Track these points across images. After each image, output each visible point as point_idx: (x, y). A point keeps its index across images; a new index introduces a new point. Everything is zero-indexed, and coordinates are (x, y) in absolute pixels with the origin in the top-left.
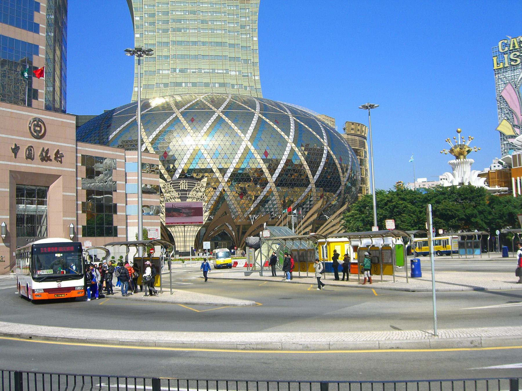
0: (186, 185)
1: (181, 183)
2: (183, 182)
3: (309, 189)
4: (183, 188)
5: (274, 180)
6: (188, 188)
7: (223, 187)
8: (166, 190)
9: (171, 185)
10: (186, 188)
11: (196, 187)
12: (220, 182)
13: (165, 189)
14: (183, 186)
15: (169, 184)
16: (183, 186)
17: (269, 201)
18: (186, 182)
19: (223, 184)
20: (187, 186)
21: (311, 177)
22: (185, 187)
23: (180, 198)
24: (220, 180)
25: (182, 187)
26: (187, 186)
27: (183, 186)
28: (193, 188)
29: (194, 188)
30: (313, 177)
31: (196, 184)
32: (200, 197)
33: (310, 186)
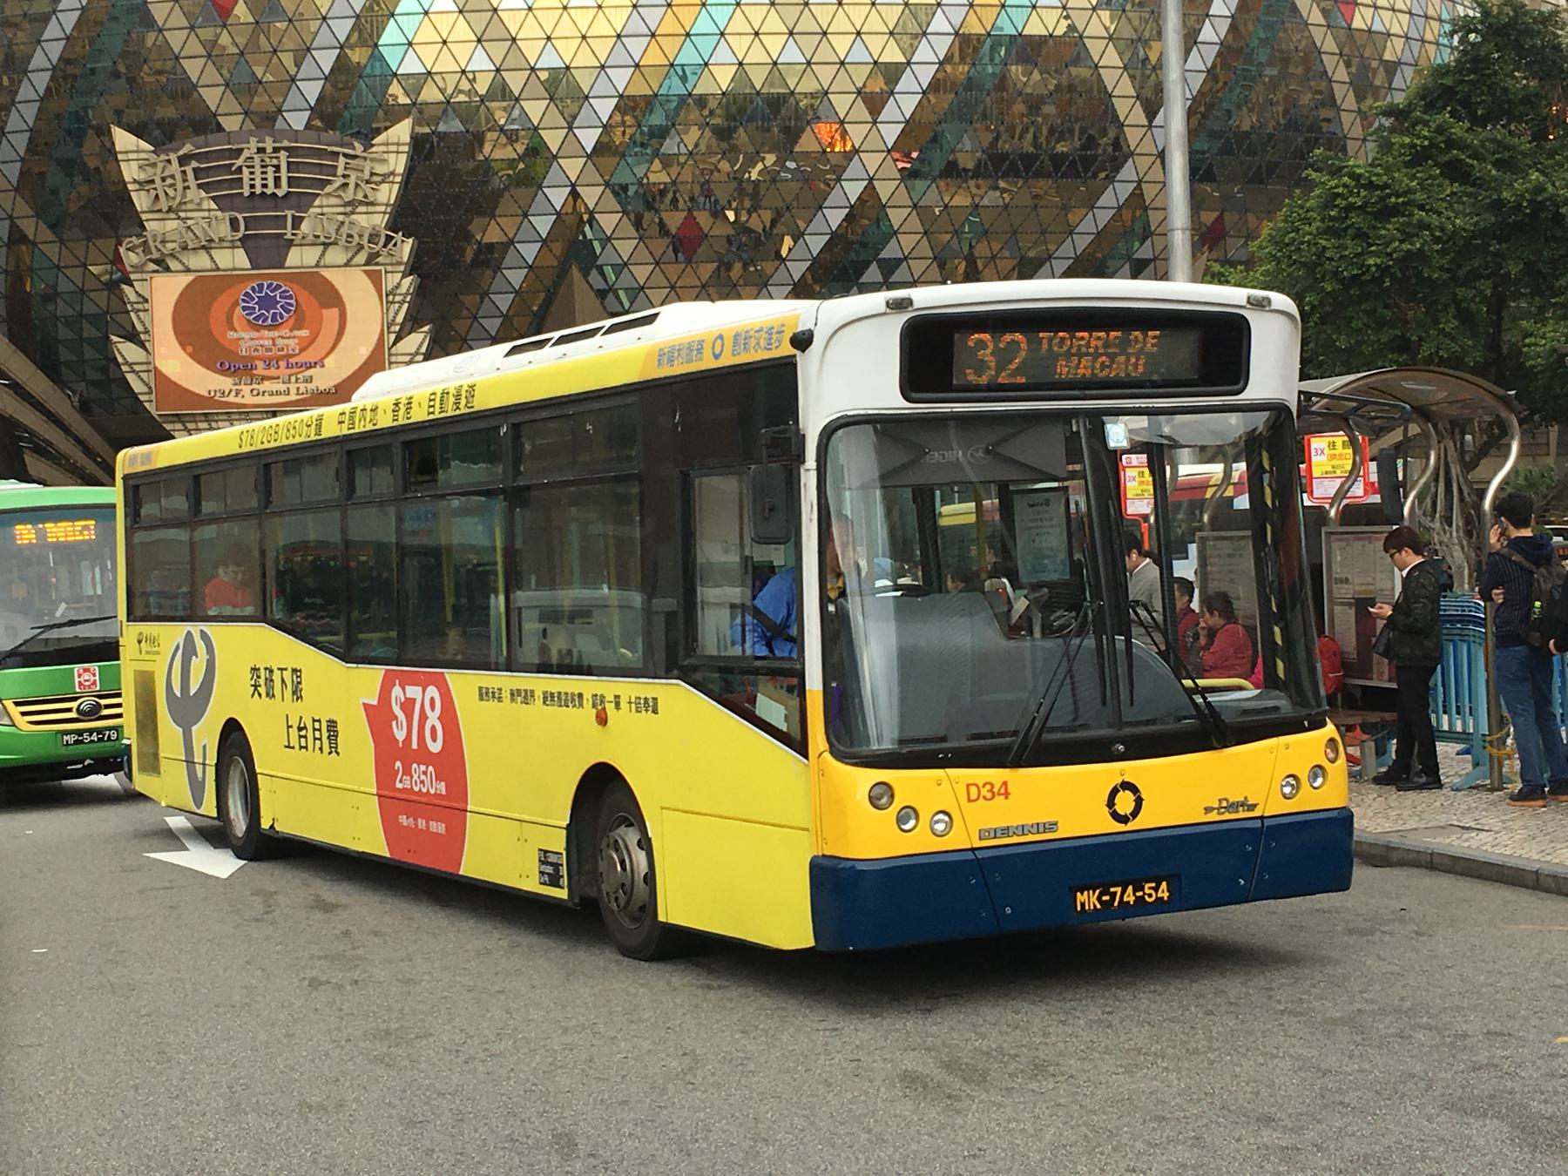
0: (277, 168)
1: (246, 154)
2: (261, 150)
3: (1124, 191)
4: (258, 183)
5: (891, 133)
6: (291, 181)
7: (573, 186)
8: (157, 196)
9: (189, 169)
10: (277, 180)
11: (339, 182)
12: (555, 157)
13: (153, 193)
14: (258, 170)
15: (175, 163)
16: (258, 176)
17: (867, 264)
18: (276, 150)
19: (573, 167)
20: (284, 174)
21: (1139, 116)
22: (271, 182)
23: (244, 241)
24: (553, 139)
25: (254, 179)
26: (284, 174)
27: (258, 176)
28: (324, 184)
29: (329, 182)
30: (1151, 122)
31: (342, 160)
32: (365, 242)
33: (1128, 172)
